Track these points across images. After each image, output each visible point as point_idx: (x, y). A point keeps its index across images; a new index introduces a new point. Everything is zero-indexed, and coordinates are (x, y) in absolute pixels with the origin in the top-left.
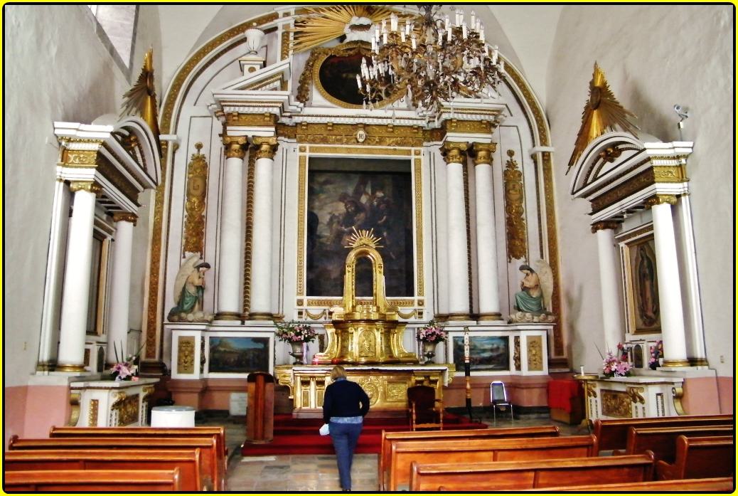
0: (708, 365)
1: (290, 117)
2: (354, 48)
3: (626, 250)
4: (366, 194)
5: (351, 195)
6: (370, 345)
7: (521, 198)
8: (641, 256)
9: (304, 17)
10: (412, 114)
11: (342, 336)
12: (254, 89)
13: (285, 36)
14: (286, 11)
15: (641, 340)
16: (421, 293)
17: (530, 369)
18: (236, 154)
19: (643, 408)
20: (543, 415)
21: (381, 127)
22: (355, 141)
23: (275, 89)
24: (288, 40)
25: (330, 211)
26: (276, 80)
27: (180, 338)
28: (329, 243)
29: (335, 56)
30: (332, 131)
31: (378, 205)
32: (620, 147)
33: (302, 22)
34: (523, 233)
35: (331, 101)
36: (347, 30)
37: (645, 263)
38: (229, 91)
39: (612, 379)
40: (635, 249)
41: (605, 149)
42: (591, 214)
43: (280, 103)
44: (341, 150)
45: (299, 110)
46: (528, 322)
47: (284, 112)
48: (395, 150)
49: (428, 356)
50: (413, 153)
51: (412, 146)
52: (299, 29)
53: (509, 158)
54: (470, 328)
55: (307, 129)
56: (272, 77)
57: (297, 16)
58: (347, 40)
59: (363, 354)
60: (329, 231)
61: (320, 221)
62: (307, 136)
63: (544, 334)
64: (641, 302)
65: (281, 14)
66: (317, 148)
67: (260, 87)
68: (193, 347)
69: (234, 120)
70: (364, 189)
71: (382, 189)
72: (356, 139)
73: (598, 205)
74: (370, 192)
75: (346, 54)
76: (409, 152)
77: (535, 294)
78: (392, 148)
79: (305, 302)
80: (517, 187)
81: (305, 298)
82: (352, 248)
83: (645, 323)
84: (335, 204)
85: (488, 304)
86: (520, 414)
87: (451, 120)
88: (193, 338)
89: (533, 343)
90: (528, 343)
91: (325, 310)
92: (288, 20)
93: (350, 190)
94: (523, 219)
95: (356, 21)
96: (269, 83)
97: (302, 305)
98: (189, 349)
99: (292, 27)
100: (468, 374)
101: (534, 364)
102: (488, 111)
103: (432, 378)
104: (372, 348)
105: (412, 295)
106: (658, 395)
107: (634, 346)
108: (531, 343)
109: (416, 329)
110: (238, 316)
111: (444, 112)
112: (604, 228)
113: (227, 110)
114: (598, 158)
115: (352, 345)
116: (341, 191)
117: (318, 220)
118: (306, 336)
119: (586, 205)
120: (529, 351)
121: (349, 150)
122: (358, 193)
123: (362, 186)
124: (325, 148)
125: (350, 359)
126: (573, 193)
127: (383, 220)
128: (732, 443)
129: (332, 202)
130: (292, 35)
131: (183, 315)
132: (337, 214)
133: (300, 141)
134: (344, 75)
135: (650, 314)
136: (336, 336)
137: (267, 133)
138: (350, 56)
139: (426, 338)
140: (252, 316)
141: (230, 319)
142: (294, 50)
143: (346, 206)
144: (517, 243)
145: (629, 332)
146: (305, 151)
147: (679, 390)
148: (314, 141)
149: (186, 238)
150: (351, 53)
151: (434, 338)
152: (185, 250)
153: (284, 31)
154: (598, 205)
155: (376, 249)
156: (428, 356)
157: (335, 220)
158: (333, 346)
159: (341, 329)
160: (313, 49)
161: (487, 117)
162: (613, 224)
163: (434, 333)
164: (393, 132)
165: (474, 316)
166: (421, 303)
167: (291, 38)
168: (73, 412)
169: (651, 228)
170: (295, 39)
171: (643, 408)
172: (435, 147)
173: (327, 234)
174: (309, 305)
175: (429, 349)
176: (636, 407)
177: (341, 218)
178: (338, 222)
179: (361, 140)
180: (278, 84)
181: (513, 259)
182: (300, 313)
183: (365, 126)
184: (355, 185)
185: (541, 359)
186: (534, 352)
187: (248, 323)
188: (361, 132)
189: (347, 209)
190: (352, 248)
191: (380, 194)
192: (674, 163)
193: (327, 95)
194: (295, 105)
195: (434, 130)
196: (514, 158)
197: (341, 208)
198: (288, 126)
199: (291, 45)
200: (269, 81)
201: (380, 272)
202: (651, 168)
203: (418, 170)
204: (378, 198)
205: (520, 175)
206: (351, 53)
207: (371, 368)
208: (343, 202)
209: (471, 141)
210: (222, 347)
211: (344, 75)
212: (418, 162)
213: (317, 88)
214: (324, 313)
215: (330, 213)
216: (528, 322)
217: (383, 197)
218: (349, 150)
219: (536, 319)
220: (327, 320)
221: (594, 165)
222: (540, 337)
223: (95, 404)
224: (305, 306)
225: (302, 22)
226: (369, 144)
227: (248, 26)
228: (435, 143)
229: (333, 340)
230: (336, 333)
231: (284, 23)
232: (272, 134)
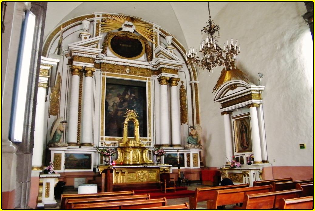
0: (268, 163)
2: (125, 34)
3: (235, 122)
4: (128, 94)
5: (122, 94)
6: (136, 157)
7: (186, 100)
8: (242, 124)
9: (106, 18)
10: (147, 63)
11: (124, 153)
12: (86, 46)
13: (98, 24)
14: (98, 15)
15: (243, 155)
16: (150, 136)
17: (194, 166)
18: (77, 73)
19: (249, 178)
20: (199, 184)
21: (135, 68)
22: (125, 72)
23: (94, 47)
24: (99, 27)
25: (113, 101)
26: (95, 44)
27: (55, 154)
28: (112, 114)
29: (117, 36)
30: (114, 68)
31: (132, 100)
32: (237, 85)
33: (105, 20)
34: (186, 113)
35: (115, 55)
36: (123, 26)
37: (244, 127)
38: (76, 46)
39: (235, 168)
40: (239, 122)
41: (231, 85)
42: (221, 108)
43: (97, 53)
44: (119, 76)
46: (193, 148)
48: (141, 77)
49: (158, 161)
50: (147, 79)
52: (103, 23)
53: (181, 84)
54: (180, 150)
56: (94, 42)
57: (103, 18)
58: (123, 30)
60: (112, 109)
61: (109, 105)
62: (105, 69)
63: (198, 153)
64: (241, 141)
65: (96, 16)
66: (109, 74)
67: (89, 46)
68: (61, 158)
69: (77, 59)
70: (127, 93)
71: (134, 93)
72: (126, 72)
73: (224, 105)
74: (129, 93)
75: (122, 36)
76: (146, 79)
77: (195, 137)
79: (104, 139)
80: (184, 96)
81: (104, 137)
82: (127, 117)
83: (243, 148)
84: (115, 98)
85: (176, 141)
86: (191, 183)
87: (164, 68)
88: (61, 154)
89: (195, 156)
90: (193, 156)
91: (112, 142)
93: (121, 93)
94: (186, 108)
95: (127, 23)
96: (92, 45)
97: (103, 140)
98: (59, 159)
99: (101, 21)
100: (179, 168)
101: (195, 164)
102: (177, 65)
103: (123, 171)
104: (137, 159)
105: (146, 137)
106: (254, 173)
107: (240, 157)
108: (194, 156)
110: (76, 144)
112: (226, 114)
113: (73, 54)
114: (228, 87)
116: (118, 93)
117: (108, 104)
119: (219, 105)
120: (193, 159)
121: (122, 76)
122: (125, 94)
123: (126, 91)
124: (113, 74)
125: (127, 163)
126: (214, 100)
127: (134, 106)
128: (312, 184)
129: (114, 97)
130: (100, 25)
131: (56, 144)
132: (116, 102)
133: (103, 70)
134: (121, 45)
135: (245, 145)
137: (91, 66)
138: (124, 37)
140: (83, 144)
141: (74, 146)
142: (101, 31)
143: (119, 99)
144: (184, 117)
145: (235, 151)
146: (104, 75)
147: (261, 171)
148: (108, 71)
149: (51, 109)
150: (124, 35)
151: (161, 154)
152: (50, 114)
153: (97, 23)
154: (224, 105)
155: (136, 117)
156: (158, 161)
157: (115, 105)
159: (124, 150)
160: (108, 32)
161: (177, 68)
162: (229, 113)
163: (161, 152)
164: (140, 70)
165: (171, 145)
166: (150, 140)
167: (100, 26)
168: (40, 189)
169: (249, 114)
170: (102, 27)
171: (249, 178)
172: (155, 78)
173: (112, 110)
174: (106, 140)
175: (158, 158)
176: (245, 178)
177: (118, 104)
178: (117, 105)
179: (127, 72)
180: (96, 45)
181: (183, 123)
182: (102, 143)
183: (130, 66)
184: (123, 90)
185: (197, 162)
186: (195, 159)
187: (82, 147)
188: (128, 69)
189: (120, 100)
190: (127, 117)
191: (133, 95)
192: (258, 93)
193: (114, 52)
195: (155, 71)
196: (183, 84)
197: (118, 100)
198: (97, 63)
199: (100, 29)
200: (93, 44)
201: (138, 127)
202: (251, 94)
203: (149, 86)
204: (133, 97)
205: (185, 91)
206: (124, 35)
207: (144, 166)
208: (119, 97)
209: (171, 76)
210: (71, 158)
212: (149, 83)
214: (112, 144)
215: (113, 102)
216: (193, 148)
217: (134, 96)
218: (122, 76)
219: (196, 147)
220: (113, 146)
221: (224, 90)
222: (197, 154)
223: (48, 184)
224: (104, 141)
225: (105, 20)
226: (131, 74)
227: (83, 18)
229: (120, 155)
232: (93, 67)
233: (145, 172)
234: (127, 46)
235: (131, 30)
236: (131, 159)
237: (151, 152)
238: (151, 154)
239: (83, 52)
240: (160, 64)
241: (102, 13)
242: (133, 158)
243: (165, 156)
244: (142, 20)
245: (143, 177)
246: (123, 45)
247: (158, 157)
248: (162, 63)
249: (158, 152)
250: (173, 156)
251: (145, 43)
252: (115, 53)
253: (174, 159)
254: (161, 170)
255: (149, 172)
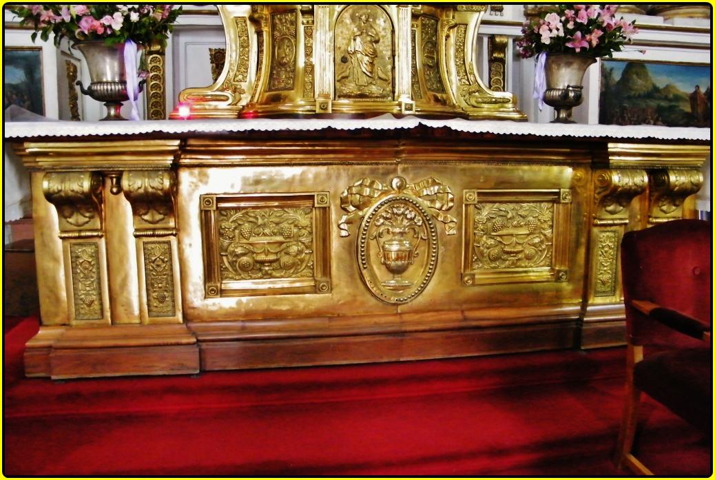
6: (375, 55)
11: (274, 27)
59: (351, 87)
109: (486, 40)
115: (309, 54)
118: (134, 17)
136: (251, 30)
139: (565, 40)
151: (594, 38)
158: (243, 65)
175: (566, 77)
229: (245, 46)
230: (252, 19)
233: (435, 189)
236: (324, 79)
237: (502, 48)
238: (502, 61)
242: (344, 60)
243: (605, 75)
245: (409, 255)
247: (569, 64)
249: (565, 24)
250: (661, 81)
253: (663, 104)
254: (616, 178)
255: (486, 198)
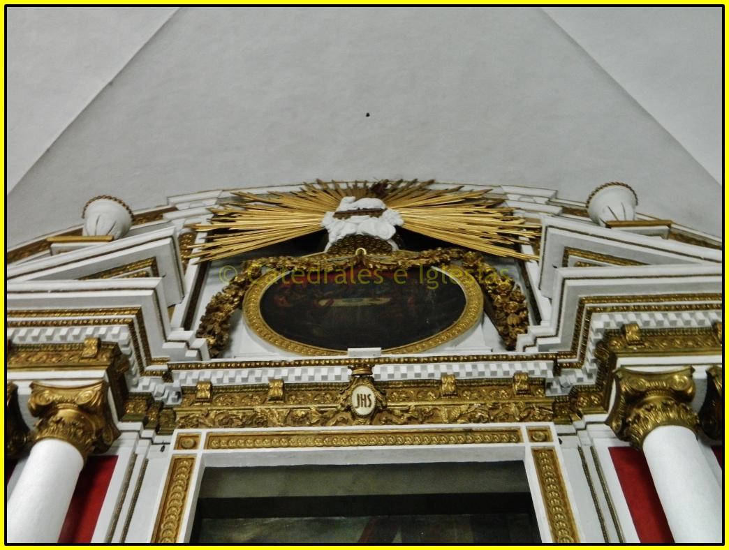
1: (167, 377)
33: (229, 215)
45: (194, 354)
47: (150, 361)
51: (522, 420)
55: (210, 401)
58: (333, 238)
72: (349, 409)
78: (458, 426)
87: (622, 330)
92: (199, 215)
95: (346, 204)
111: (594, 310)
134: (323, 303)
170: (208, 240)
179: (361, 411)
194: (177, 340)
203: (552, 478)
211: (323, 303)
212: (546, 460)
213: (251, 325)
226: (388, 422)
228: (588, 418)
231: (189, 222)
234: (366, 301)
235: (383, 228)
239: (39, 313)
240: (589, 313)
241: (216, 194)
244: (432, 187)
246: (340, 303)
248: (600, 299)
251: (474, 271)
252: (287, 341)
